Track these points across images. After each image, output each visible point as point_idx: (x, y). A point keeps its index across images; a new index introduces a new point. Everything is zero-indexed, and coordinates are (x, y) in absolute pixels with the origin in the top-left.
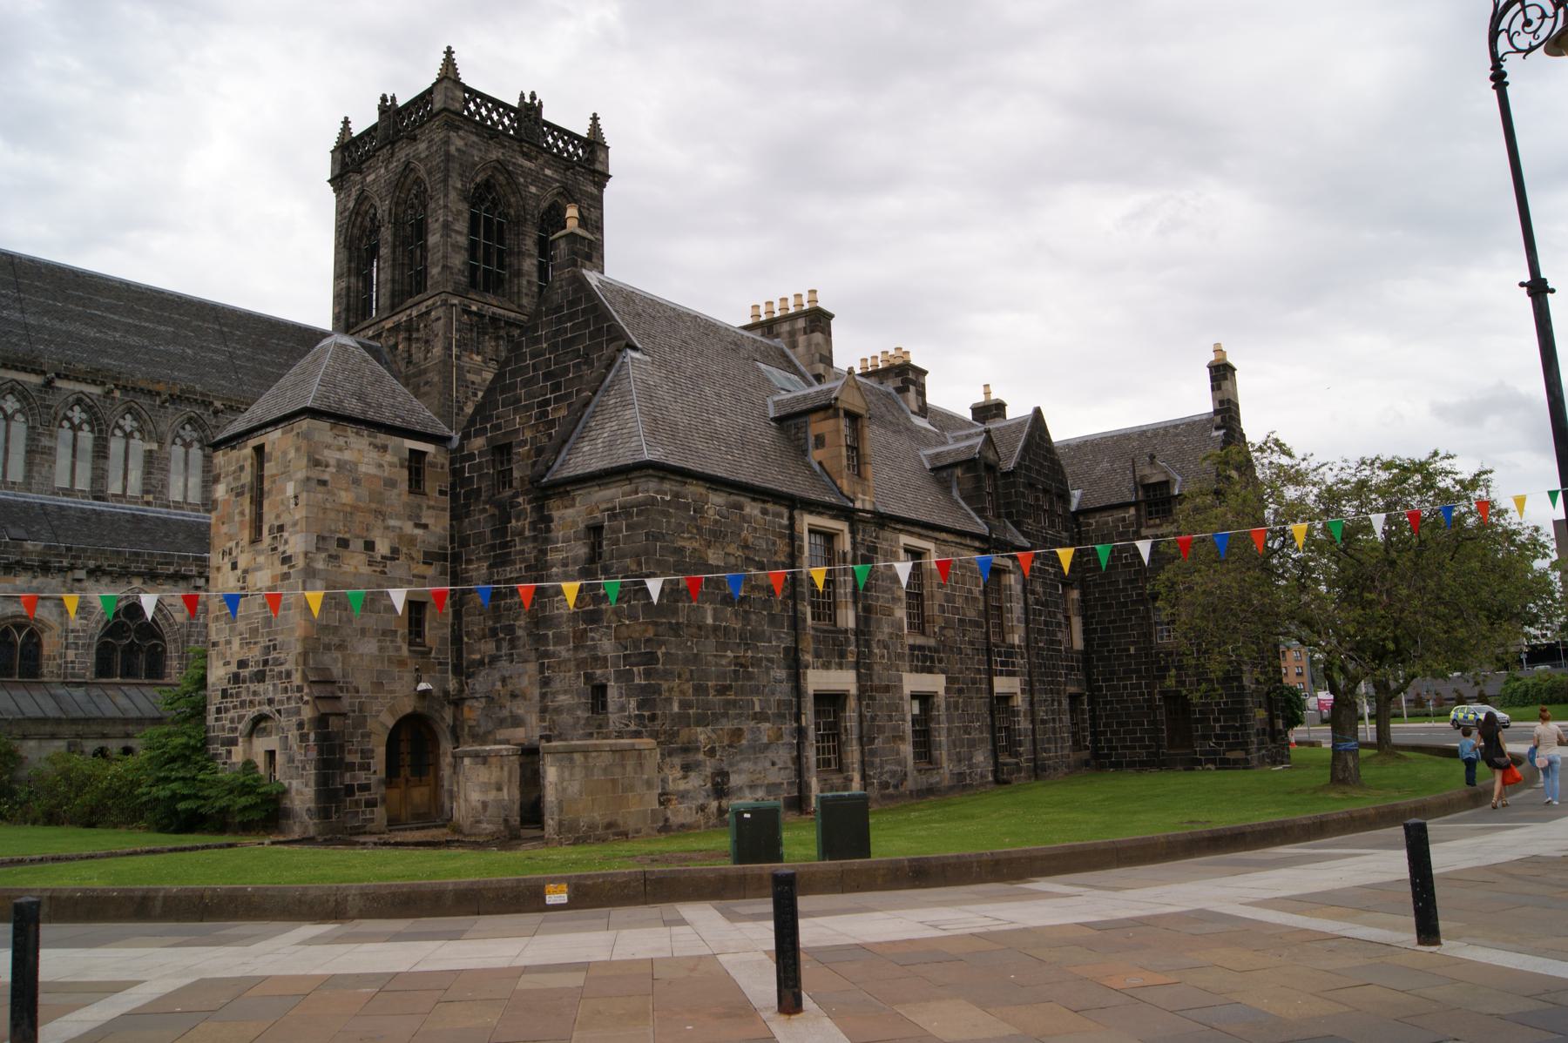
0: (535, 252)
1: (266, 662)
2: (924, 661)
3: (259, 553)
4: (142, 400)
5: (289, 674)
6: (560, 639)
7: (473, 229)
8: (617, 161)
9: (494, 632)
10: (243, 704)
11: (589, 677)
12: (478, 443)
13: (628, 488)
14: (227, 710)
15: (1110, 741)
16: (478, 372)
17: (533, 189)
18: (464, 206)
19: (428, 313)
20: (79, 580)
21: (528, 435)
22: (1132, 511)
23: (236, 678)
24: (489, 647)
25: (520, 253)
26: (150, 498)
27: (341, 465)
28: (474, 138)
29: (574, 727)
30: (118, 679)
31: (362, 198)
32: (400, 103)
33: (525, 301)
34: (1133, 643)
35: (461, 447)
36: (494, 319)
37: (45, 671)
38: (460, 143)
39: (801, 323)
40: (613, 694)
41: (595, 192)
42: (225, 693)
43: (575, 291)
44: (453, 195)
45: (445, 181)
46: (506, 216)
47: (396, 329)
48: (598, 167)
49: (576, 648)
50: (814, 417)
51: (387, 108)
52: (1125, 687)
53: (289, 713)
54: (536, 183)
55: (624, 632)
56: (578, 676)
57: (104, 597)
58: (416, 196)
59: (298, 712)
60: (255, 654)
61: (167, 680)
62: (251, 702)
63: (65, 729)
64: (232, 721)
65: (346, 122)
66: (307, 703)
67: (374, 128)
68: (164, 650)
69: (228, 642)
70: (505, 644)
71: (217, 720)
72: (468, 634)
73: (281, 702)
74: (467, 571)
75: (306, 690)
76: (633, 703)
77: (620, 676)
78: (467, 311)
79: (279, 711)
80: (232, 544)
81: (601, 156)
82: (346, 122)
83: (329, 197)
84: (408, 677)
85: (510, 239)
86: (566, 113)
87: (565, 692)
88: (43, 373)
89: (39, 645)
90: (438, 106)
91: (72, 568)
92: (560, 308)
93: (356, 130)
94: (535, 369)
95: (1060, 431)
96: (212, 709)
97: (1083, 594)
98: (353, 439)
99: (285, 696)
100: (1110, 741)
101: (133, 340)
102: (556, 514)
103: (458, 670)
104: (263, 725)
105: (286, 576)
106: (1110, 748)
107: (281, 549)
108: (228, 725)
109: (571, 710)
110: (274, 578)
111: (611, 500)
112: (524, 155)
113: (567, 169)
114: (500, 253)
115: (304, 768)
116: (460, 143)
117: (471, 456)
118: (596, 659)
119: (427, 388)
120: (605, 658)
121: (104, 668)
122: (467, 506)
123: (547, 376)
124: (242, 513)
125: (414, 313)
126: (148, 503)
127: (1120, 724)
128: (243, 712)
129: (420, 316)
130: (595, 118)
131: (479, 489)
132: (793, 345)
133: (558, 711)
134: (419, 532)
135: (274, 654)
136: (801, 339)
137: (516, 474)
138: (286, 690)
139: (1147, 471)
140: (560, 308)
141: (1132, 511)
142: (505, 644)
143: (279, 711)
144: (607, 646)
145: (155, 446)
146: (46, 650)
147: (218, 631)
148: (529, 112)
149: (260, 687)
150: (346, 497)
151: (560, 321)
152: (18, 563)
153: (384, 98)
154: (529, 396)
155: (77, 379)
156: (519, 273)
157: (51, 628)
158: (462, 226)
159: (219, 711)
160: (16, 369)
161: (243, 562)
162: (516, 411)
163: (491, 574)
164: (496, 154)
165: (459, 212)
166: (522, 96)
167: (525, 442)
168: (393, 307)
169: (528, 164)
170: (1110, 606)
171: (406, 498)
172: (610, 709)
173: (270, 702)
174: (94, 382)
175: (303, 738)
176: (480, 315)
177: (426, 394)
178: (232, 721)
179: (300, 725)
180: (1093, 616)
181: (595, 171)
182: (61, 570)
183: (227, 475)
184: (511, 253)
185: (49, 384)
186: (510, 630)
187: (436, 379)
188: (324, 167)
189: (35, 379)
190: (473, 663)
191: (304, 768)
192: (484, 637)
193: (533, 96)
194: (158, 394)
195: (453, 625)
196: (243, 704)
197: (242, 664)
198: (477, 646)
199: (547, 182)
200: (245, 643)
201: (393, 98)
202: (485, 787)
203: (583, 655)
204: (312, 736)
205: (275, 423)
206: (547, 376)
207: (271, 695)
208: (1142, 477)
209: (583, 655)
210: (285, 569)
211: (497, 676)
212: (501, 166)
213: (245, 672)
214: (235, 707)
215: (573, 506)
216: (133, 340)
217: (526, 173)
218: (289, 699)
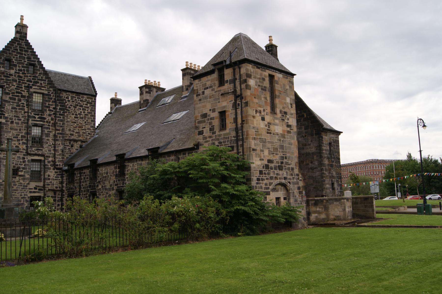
1: (282, 163)
5: (293, 169)
10: (271, 178)
11: (332, 181)
14: (263, 180)
23: (267, 167)
42: (261, 172)
53: (294, 183)
59: (298, 183)
60: (276, 158)
62: (276, 178)
64: (266, 184)
66: (301, 180)
69: (262, 151)
71: (257, 183)
73: (290, 179)
79: (289, 182)
80: (262, 109)
96: (254, 178)
99: (291, 177)
102: (324, 137)
105: (289, 132)
107: (286, 121)
108: (264, 186)
124: (266, 98)
128: (272, 181)
135: (285, 161)
138: (292, 175)
143: (289, 182)
147: (255, 145)
149: (280, 172)
159: (258, 180)
161: (268, 118)
173: (285, 178)
175: (300, 193)
178: (266, 184)
179: (299, 188)
191: (301, 204)
196: (271, 178)
197: (270, 161)
200: (270, 153)
204: (304, 192)
207: (285, 176)
210: (289, 129)
213: (271, 165)
214: (267, 179)
218: (293, 178)
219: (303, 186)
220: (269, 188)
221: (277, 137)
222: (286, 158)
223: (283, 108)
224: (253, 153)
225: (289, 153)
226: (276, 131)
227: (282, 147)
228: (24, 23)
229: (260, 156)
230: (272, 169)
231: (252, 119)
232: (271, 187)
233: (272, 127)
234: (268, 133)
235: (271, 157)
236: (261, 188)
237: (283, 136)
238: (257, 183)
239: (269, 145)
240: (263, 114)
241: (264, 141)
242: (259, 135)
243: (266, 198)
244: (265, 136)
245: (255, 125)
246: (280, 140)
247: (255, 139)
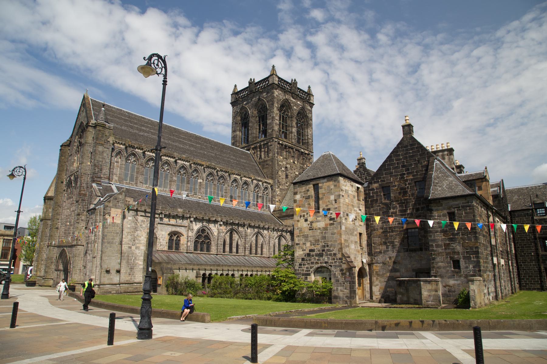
0: (296, 126)
3: (318, 217)
4: (198, 167)
6: (437, 246)
7: (280, 120)
9: (385, 243)
10: (312, 263)
12: (375, 186)
13: (464, 201)
15: (526, 281)
16: (282, 162)
17: (295, 108)
18: (278, 112)
19: (267, 143)
20: (191, 221)
21: (397, 183)
22: (531, 211)
23: (309, 255)
24: (384, 247)
25: (292, 127)
26: (200, 196)
27: (346, 191)
28: (280, 92)
29: (447, 272)
30: (199, 252)
31: (243, 108)
32: (256, 81)
33: (293, 141)
34: (533, 252)
35: (368, 186)
36: (286, 146)
37: (181, 248)
38: (277, 93)
39: (446, 153)
40: (462, 263)
41: (309, 108)
42: (303, 259)
43: (413, 141)
44: (275, 109)
45: (273, 104)
46: (287, 115)
48: (311, 101)
49: (445, 249)
50: (477, 181)
51: (251, 83)
52: (531, 265)
55: (466, 245)
56: (447, 257)
57: (196, 226)
58: (261, 108)
59: (341, 266)
60: (318, 248)
61: (211, 253)
62: (316, 263)
63: (196, 267)
65: (236, 86)
67: (247, 88)
68: (211, 244)
69: (304, 244)
70: (390, 248)
72: (374, 243)
74: (372, 224)
75: (344, 259)
76: (471, 266)
77: (464, 258)
78: (279, 144)
79: (331, 266)
81: (312, 98)
82: (236, 86)
83: (230, 108)
84: (360, 256)
85: (289, 122)
86: (302, 86)
87: (442, 262)
88: (175, 158)
89: (179, 240)
90: (270, 82)
91: (190, 217)
92: (407, 146)
93: (239, 89)
94: (398, 163)
95: (507, 187)
97: (513, 236)
98: (347, 183)
99: (333, 261)
100: (526, 281)
101: (192, 149)
103: (370, 254)
104: (320, 269)
105: (331, 224)
106: (526, 284)
107: (329, 216)
108: (305, 269)
109: (444, 267)
110: (326, 225)
111: (458, 205)
112: (293, 98)
114: (286, 126)
115: (344, 283)
116: (277, 93)
117: (373, 189)
118: (454, 253)
119: (267, 166)
120: (459, 252)
121: (196, 249)
122: (372, 204)
123: (403, 166)
124: (309, 204)
125: (262, 143)
126: (200, 198)
127: (529, 276)
129: (264, 145)
130: (309, 87)
131: (377, 199)
132: (444, 159)
133: (439, 268)
134: (360, 212)
136: (446, 157)
137: (392, 195)
138: (334, 259)
139: (535, 199)
140: (407, 146)
141: (531, 211)
142: (390, 248)
143: (331, 266)
144: (459, 248)
145: (202, 181)
146: (182, 242)
147: (299, 240)
150: (347, 201)
151: (407, 150)
152: (177, 215)
153: (251, 80)
154: (396, 172)
155: (183, 160)
156: (292, 132)
157: (183, 235)
158: (277, 118)
160: (168, 156)
161: (310, 219)
162: (391, 176)
163: (383, 226)
165: (277, 114)
166: (292, 80)
167: (396, 186)
169: (293, 100)
170: (524, 240)
171: (357, 201)
172: (461, 268)
173: (326, 263)
174: (187, 161)
176: (282, 145)
177: (267, 168)
178: (307, 268)
179: (342, 270)
180: (518, 243)
181: (310, 103)
182: (187, 218)
183: (301, 192)
184: (289, 126)
185: (176, 162)
186: (392, 243)
187: (271, 163)
188: (229, 99)
189: (172, 160)
190: (376, 253)
191: (344, 283)
192: (381, 244)
193: (295, 80)
194: (203, 165)
195: (367, 241)
196: (312, 263)
197: (311, 250)
198: (378, 247)
199: (298, 105)
201: (254, 80)
202: (430, 291)
203: (448, 251)
204: (348, 274)
205: (324, 177)
206: (403, 166)
208: (534, 201)
209: (448, 251)
211: (387, 256)
212: (287, 101)
215: (442, 206)
216: (192, 149)
217: (293, 103)
219: (346, 269)
220: (309, 271)
221: (319, 231)
222: (328, 246)
223: (327, 206)
224: (297, 247)
225: (331, 241)
226: (319, 226)
227: (324, 238)
228: (362, 156)
229: (302, 248)
230: (313, 256)
231: (297, 222)
232: (311, 270)
233: (314, 225)
234: (310, 230)
235: (313, 247)
236: (303, 270)
237: (325, 229)
238: (299, 267)
239: (311, 239)
240: (306, 216)
241: (306, 237)
242: (302, 233)
243: (307, 278)
244: (307, 232)
245: (299, 226)
246: (322, 233)
247: (298, 236)
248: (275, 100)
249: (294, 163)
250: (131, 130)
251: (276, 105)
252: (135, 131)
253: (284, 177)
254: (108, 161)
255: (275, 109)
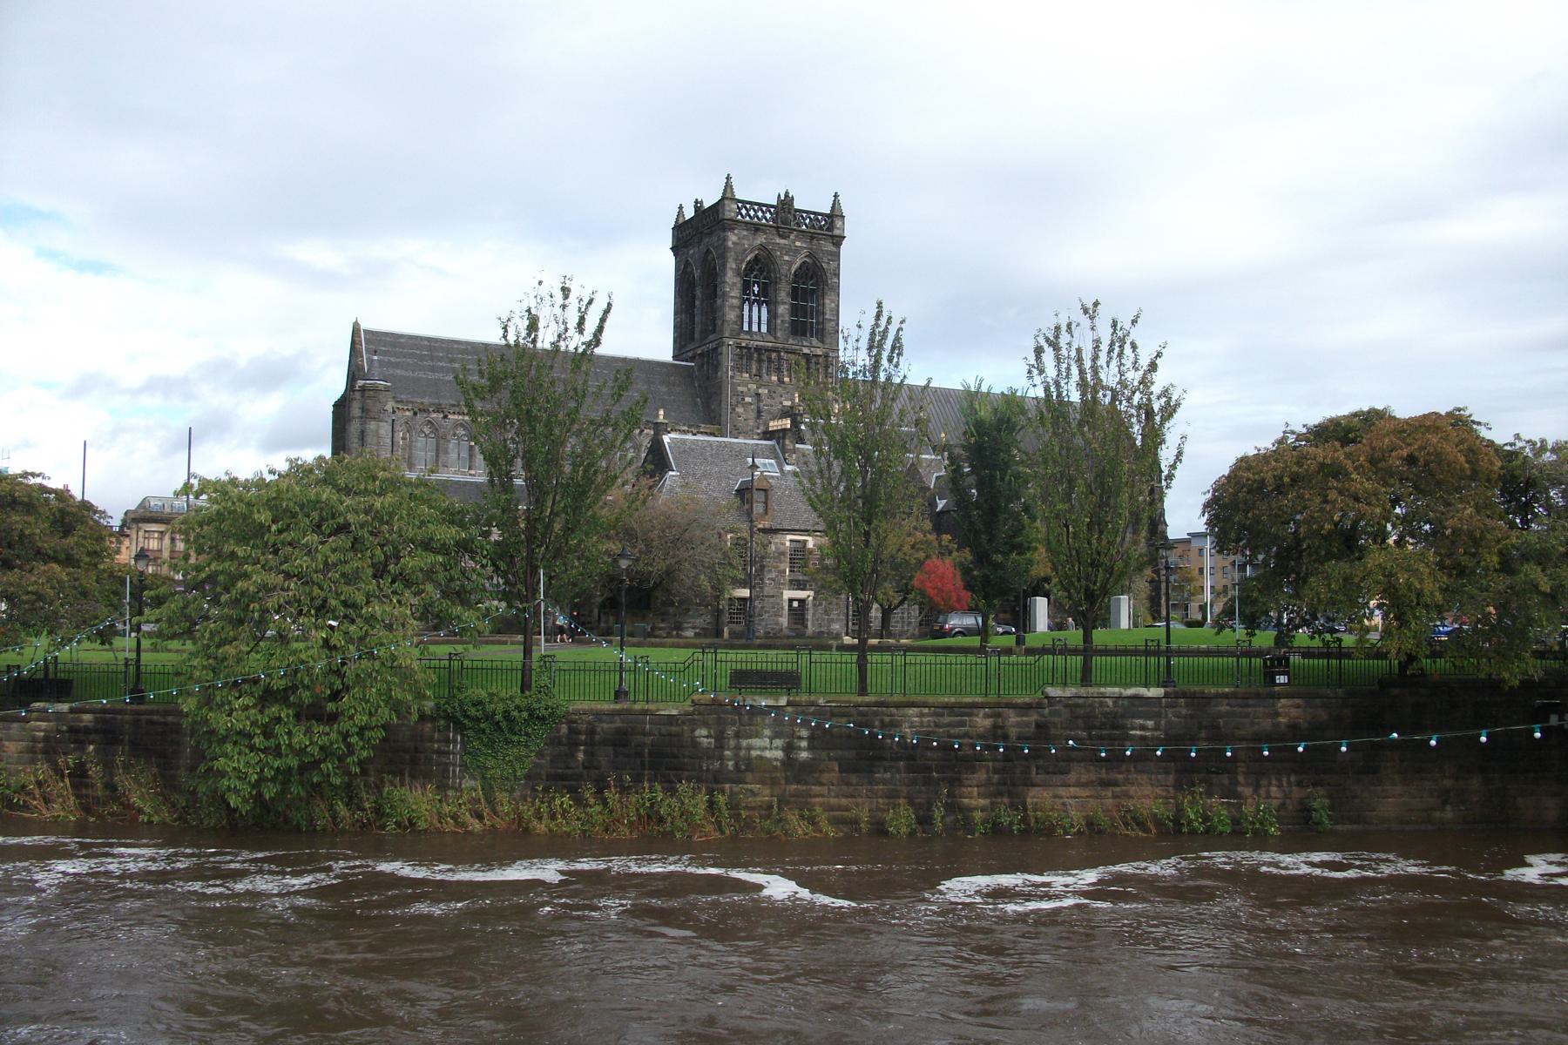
2: (800, 585)
8: (851, 228)
31: (687, 264)
32: (706, 206)
36: (757, 349)
41: (832, 248)
45: (724, 265)
47: (701, 355)
48: (836, 232)
51: (698, 205)
54: (791, 256)
81: (838, 223)
86: (811, 201)
112: (781, 237)
113: (812, 238)
148: (786, 203)
164: (761, 239)
168: (702, 339)
169: (783, 241)
199: (797, 251)
212: (762, 247)
217: (781, 248)
248: (731, 256)
249: (781, 381)
250: (431, 375)
251: (731, 265)
252: (437, 375)
253: (752, 415)
254: (389, 441)
255: (730, 274)
